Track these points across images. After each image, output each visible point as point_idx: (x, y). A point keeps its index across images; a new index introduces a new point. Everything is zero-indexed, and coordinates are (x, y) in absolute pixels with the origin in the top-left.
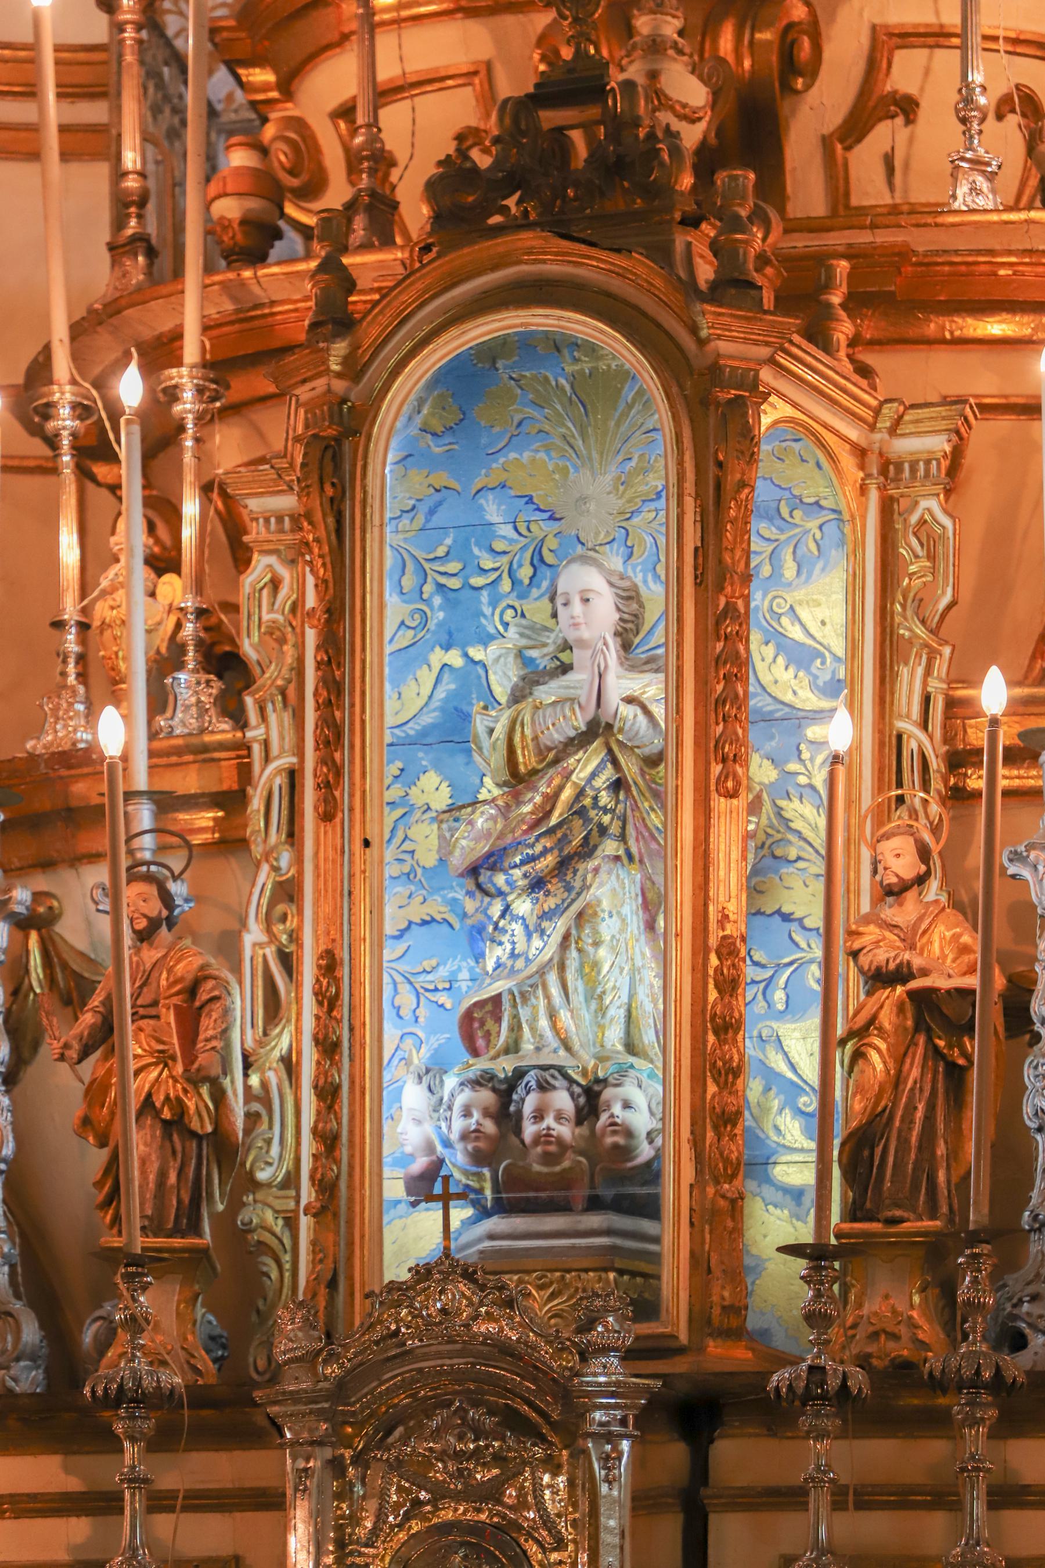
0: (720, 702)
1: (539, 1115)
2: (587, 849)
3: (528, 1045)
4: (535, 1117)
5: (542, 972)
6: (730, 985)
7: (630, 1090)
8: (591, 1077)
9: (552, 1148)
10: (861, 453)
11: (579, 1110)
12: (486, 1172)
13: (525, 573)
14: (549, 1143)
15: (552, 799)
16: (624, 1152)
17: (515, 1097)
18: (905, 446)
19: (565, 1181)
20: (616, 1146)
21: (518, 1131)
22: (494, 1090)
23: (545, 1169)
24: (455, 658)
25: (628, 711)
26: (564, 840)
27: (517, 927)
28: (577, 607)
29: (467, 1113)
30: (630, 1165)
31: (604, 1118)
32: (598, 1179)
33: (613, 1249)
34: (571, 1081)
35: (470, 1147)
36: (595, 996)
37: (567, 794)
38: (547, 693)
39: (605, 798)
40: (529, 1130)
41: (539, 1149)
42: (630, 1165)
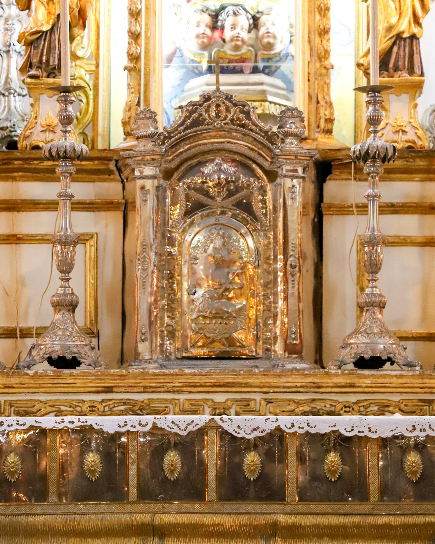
1: (233, 27)
4: (232, 28)
8: (256, 11)
9: (239, 43)
11: (250, 25)
12: (206, 53)
14: (238, 40)
17: (220, 18)
20: (269, 43)
22: (210, 15)
23: (234, 53)
30: (273, 52)
32: (259, 58)
34: (247, 12)
35: (200, 41)
41: (233, 43)
42: (273, 52)
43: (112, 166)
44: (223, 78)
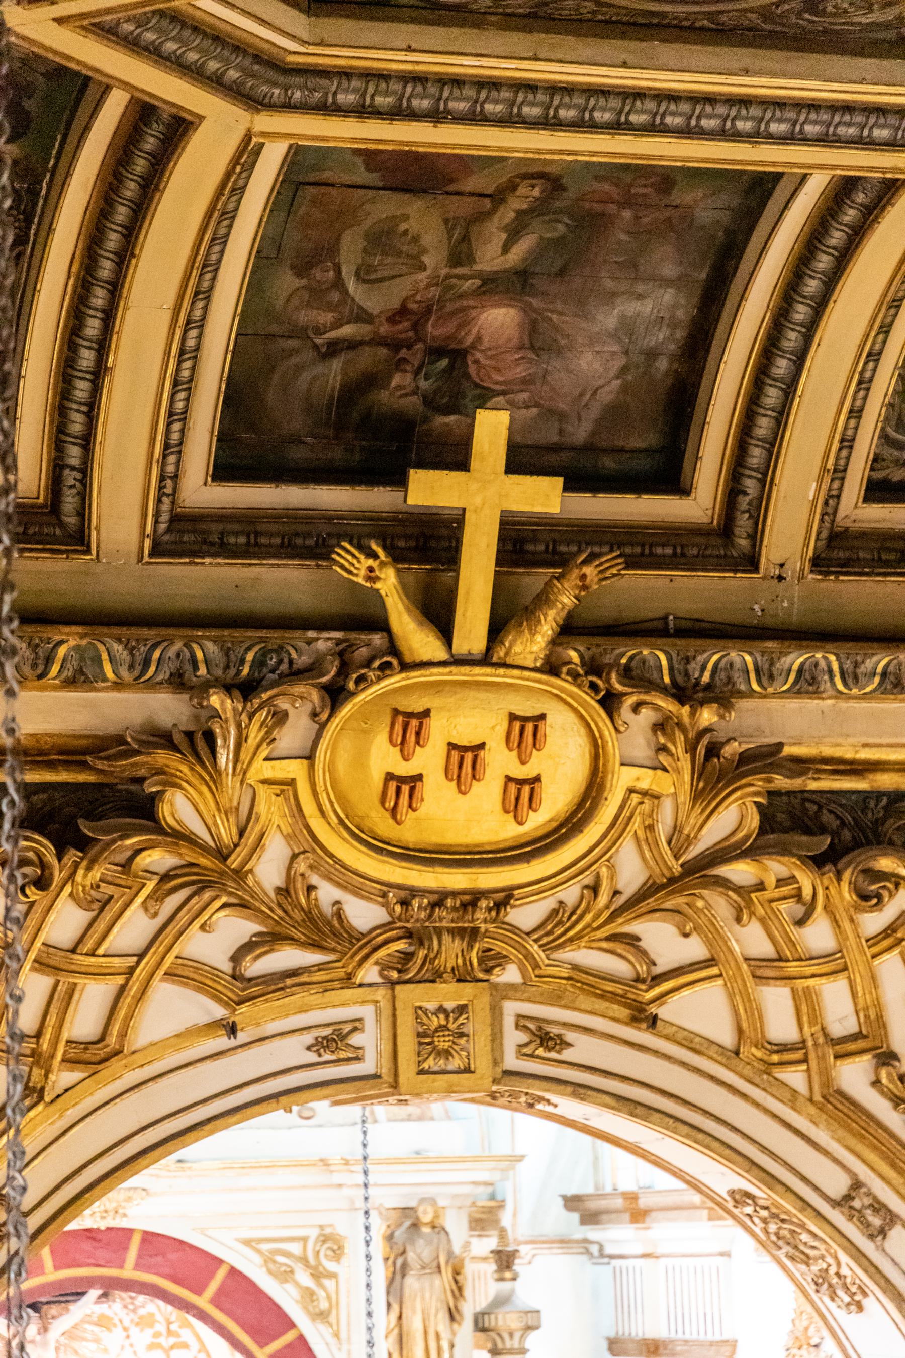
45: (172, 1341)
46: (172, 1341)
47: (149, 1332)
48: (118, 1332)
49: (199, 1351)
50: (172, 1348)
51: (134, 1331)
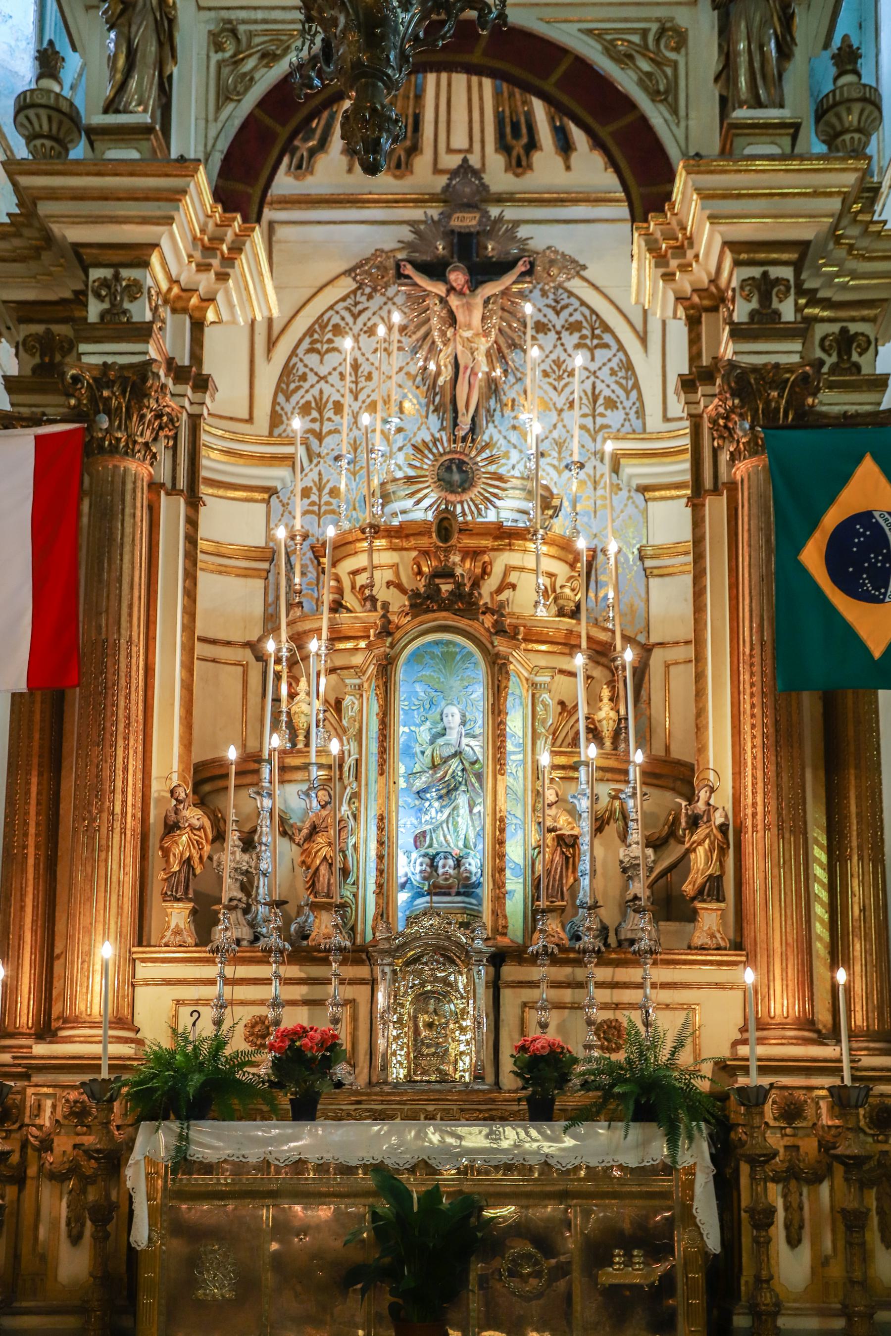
0: (499, 748)
1: (444, 867)
2: (456, 789)
3: (435, 845)
5: (441, 824)
6: (502, 830)
7: (470, 860)
10: (527, 680)
13: (428, 706)
15: (446, 773)
16: (468, 878)
18: (538, 679)
19: (450, 887)
21: (436, 871)
24: (406, 729)
25: (467, 748)
26: (449, 785)
27: (433, 811)
28: (450, 718)
29: (421, 865)
31: (463, 868)
33: (465, 908)
36: (456, 830)
37: (451, 771)
38: (441, 741)
39: (460, 774)
40: (441, 871)
43: (364, 956)
44: (435, 898)
45: (595, 342)
46: (595, 342)
47: (577, 335)
48: (552, 335)
49: (618, 351)
50: (596, 347)
51: (565, 334)
